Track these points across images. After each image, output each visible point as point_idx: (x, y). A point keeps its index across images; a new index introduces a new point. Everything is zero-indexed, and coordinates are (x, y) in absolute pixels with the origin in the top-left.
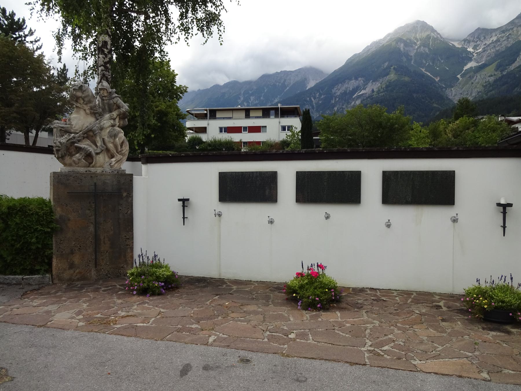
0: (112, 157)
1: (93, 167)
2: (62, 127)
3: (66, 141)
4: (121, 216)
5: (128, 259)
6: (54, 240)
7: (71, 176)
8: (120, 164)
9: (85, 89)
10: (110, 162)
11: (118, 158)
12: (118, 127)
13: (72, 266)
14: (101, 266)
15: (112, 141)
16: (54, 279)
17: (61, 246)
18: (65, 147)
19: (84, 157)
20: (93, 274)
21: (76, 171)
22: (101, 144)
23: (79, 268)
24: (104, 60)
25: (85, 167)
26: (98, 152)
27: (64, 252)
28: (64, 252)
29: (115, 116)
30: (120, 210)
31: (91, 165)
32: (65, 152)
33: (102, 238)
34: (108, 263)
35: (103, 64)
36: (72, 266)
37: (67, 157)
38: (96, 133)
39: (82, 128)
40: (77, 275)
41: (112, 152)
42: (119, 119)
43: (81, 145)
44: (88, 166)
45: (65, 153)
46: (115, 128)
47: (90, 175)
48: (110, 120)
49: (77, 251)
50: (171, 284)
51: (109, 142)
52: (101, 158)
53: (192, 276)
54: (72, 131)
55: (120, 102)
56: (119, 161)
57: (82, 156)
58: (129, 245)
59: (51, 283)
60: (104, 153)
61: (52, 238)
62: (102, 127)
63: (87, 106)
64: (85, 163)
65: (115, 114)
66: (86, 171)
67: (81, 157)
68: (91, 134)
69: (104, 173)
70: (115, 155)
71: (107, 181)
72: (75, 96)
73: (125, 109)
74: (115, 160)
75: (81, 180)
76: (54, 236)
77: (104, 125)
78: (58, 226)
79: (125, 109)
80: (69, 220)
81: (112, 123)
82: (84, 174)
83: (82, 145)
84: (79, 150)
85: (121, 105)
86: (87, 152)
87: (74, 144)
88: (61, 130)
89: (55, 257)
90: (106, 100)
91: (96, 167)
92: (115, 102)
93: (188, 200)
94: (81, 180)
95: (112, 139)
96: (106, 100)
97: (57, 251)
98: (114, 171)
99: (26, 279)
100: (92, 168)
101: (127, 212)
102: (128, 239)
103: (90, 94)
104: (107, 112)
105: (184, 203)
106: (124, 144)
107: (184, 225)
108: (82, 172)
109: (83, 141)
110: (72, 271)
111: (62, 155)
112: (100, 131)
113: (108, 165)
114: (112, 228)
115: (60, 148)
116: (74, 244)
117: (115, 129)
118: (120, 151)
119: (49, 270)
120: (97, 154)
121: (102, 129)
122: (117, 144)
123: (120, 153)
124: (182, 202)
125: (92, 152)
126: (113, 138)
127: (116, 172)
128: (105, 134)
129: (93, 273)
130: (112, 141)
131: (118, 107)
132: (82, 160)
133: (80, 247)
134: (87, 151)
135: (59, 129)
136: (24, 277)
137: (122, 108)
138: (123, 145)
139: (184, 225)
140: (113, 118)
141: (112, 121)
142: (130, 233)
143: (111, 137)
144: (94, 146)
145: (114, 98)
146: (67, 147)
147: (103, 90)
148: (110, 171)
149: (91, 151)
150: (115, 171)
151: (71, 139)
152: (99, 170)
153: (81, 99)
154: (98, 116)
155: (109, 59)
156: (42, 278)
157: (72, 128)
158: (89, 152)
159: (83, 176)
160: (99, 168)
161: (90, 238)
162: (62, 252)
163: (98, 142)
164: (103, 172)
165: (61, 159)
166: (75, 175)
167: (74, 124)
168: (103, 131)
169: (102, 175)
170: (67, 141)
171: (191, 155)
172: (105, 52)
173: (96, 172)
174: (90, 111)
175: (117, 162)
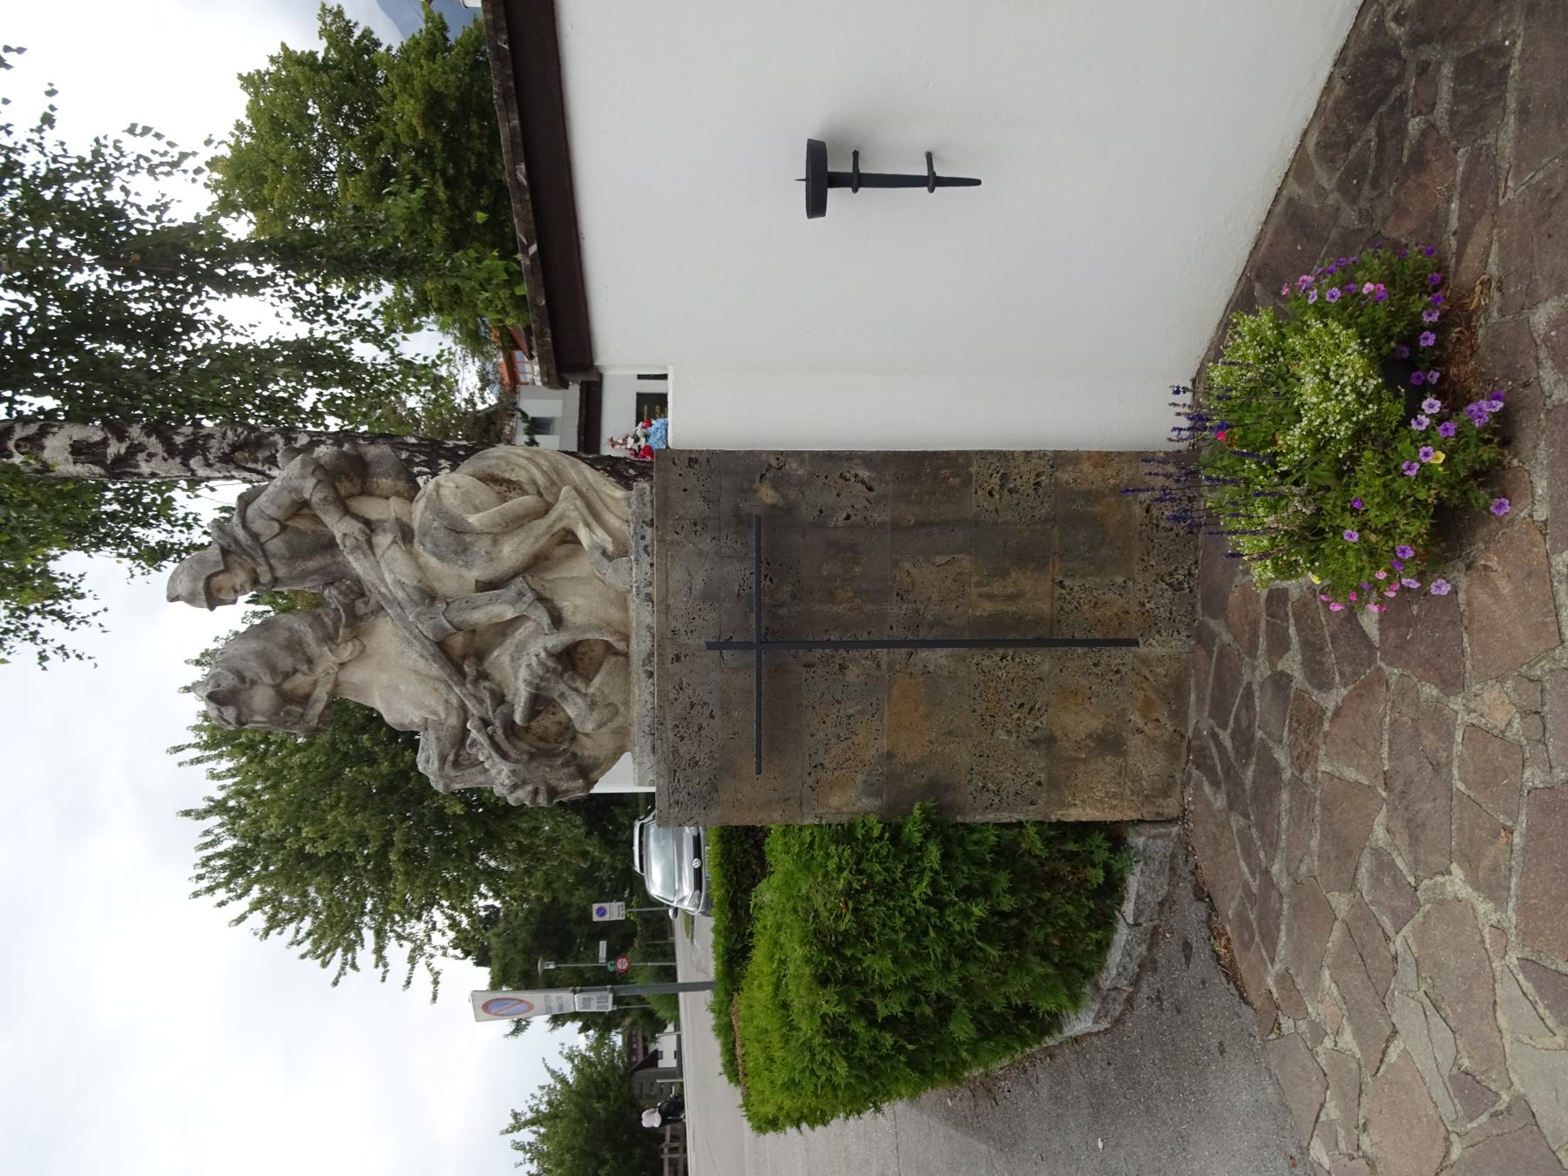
0: (568, 538)
1: (626, 638)
2: (443, 760)
3: (504, 762)
4: (882, 515)
5: (1112, 481)
6: (979, 818)
7: (675, 752)
8: (608, 500)
9: (231, 676)
10: (597, 555)
11: (574, 514)
12: (411, 499)
13: (1110, 743)
14: (1127, 612)
15: (484, 545)
16: (1158, 814)
17: (1012, 790)
18: (534, 764)
19: (579, 684)
20: (1160, 651)
21: (648, 720)
23: (1124, 709)
24: (159, 458)
25: (627, 682)
26: (545, 620)
27: (1043, 777)
28: (1043, 777)
29: (354, 527)
30: (848, 518)
31: (620, 646)
33: (988, 607)
34: (1119, 580)
35: (178, 460)
36: (1110, 743)
37: (583, 748)
38: (448, 626)
39: (438, 679)
40: (1157, 720)
41: (543, 541)
42: (371, 494)
43: (517, 690)
44: (622, 659)
45: (565, 765)
46: (416, 525)
47: (668, 665)
48: (379, 552)
49: (1044, 719)
50: (1417, 328)
51: (490, 557)
52: (579, 601)
53: (1305, 134)
54: (453, 720)
55: (272, 502)
56: (589, 506)
57: (574, 694)
58: (1038, 475)
59: (1175, 830)
60: (548, 581)
61: (971, 829)
62: (416, 597)
63: (321, 656)
64: (610, 673)
65: (340, 527)
66: (651, 675)
67: (579, 700)
68: (458, 642)
69: (653, 590)
70: (559, 526)
71: (699, 584)
72: (276, 713)
73: (303, 477)
74: (588, 525)
75: (692, 705)
76: (959, 819)
77: (402, 585)
78: (917, 812)
79: (303, 477)
80: (890, 756)
81: (394, 542)
82: (662, 694)
83: (520, 695)
84: (540, 702)
85: (286, 499)
86: (554, 671)
87: (514, 722)
88: (456, 764)
89: (1060, 812)
90: (272, 568)
91: (626, 623)
92: (276, 526)
93: (817, 153)
94: (692, 705)
95: (471, 544)
96: (272, 568)
97: (1032, 804)
98: (643, 543)
99: (1138, 913)
100: (633, 642)
101: (863, 482)
102: (1004, 477)
103: (254, 645)
104: (340, 559)
105: (838, 180)
106: (497, 472)
107: (977, 182)
108: (652, 694)
109: (498, 677)
110: (1134, 743)
111: (572, 778)
112: (441, 606)
113: (616, 570)
114: (939, 560)
115: (542, 788)
116: (1009, 732)
117: (422, 524)
118: (540, 494)
119: (1114, 834)
120: (557, 621)
121: (428, 596)
122: (498, 520)
123: (550, 499)
124: (834, 195)
125: (549, 645)
126: (468, 538)
127: (649, 532)
128: (454, 577)
129: (1154, 648)
130: (484, 545)
131: (300, 509)
132: (591, 690)
133: (1022, 705)
134: (548, 670)
135: (453, 774)
136: (1131, 921)
137: (299, 491)
138: (507, 476)
139: (977, 182)
140: (362, 538)
141: (383, 540)
142: (972, 470)
143: (465, 550)
144: (520, 634)
145: (255, 536)
146: (532, 756)
147: (219, 590)
148: (646, 560)
149: (543, 654)
150: (643, 537)
151: (491, 738)
152: (642, 617)
153: (287, 686)
154: (367, 603)
156: (1146, 864)
157: (442, 724)
158: (551, 663)
159: (672, 696)
160: (632, 614)
161: (986, 662)
162: (1039, 784)
163: (499, 616)
164: (649, 598)
165: (593, 775)
166: (671, 735)
167: (417, 713)
168: (436, 585)
169: (668, 606)
170: (504, 755)
171: (516, 122)
172: (123, 451)
173: (649, 628)
174: (346, 641)
175: (596, 515)
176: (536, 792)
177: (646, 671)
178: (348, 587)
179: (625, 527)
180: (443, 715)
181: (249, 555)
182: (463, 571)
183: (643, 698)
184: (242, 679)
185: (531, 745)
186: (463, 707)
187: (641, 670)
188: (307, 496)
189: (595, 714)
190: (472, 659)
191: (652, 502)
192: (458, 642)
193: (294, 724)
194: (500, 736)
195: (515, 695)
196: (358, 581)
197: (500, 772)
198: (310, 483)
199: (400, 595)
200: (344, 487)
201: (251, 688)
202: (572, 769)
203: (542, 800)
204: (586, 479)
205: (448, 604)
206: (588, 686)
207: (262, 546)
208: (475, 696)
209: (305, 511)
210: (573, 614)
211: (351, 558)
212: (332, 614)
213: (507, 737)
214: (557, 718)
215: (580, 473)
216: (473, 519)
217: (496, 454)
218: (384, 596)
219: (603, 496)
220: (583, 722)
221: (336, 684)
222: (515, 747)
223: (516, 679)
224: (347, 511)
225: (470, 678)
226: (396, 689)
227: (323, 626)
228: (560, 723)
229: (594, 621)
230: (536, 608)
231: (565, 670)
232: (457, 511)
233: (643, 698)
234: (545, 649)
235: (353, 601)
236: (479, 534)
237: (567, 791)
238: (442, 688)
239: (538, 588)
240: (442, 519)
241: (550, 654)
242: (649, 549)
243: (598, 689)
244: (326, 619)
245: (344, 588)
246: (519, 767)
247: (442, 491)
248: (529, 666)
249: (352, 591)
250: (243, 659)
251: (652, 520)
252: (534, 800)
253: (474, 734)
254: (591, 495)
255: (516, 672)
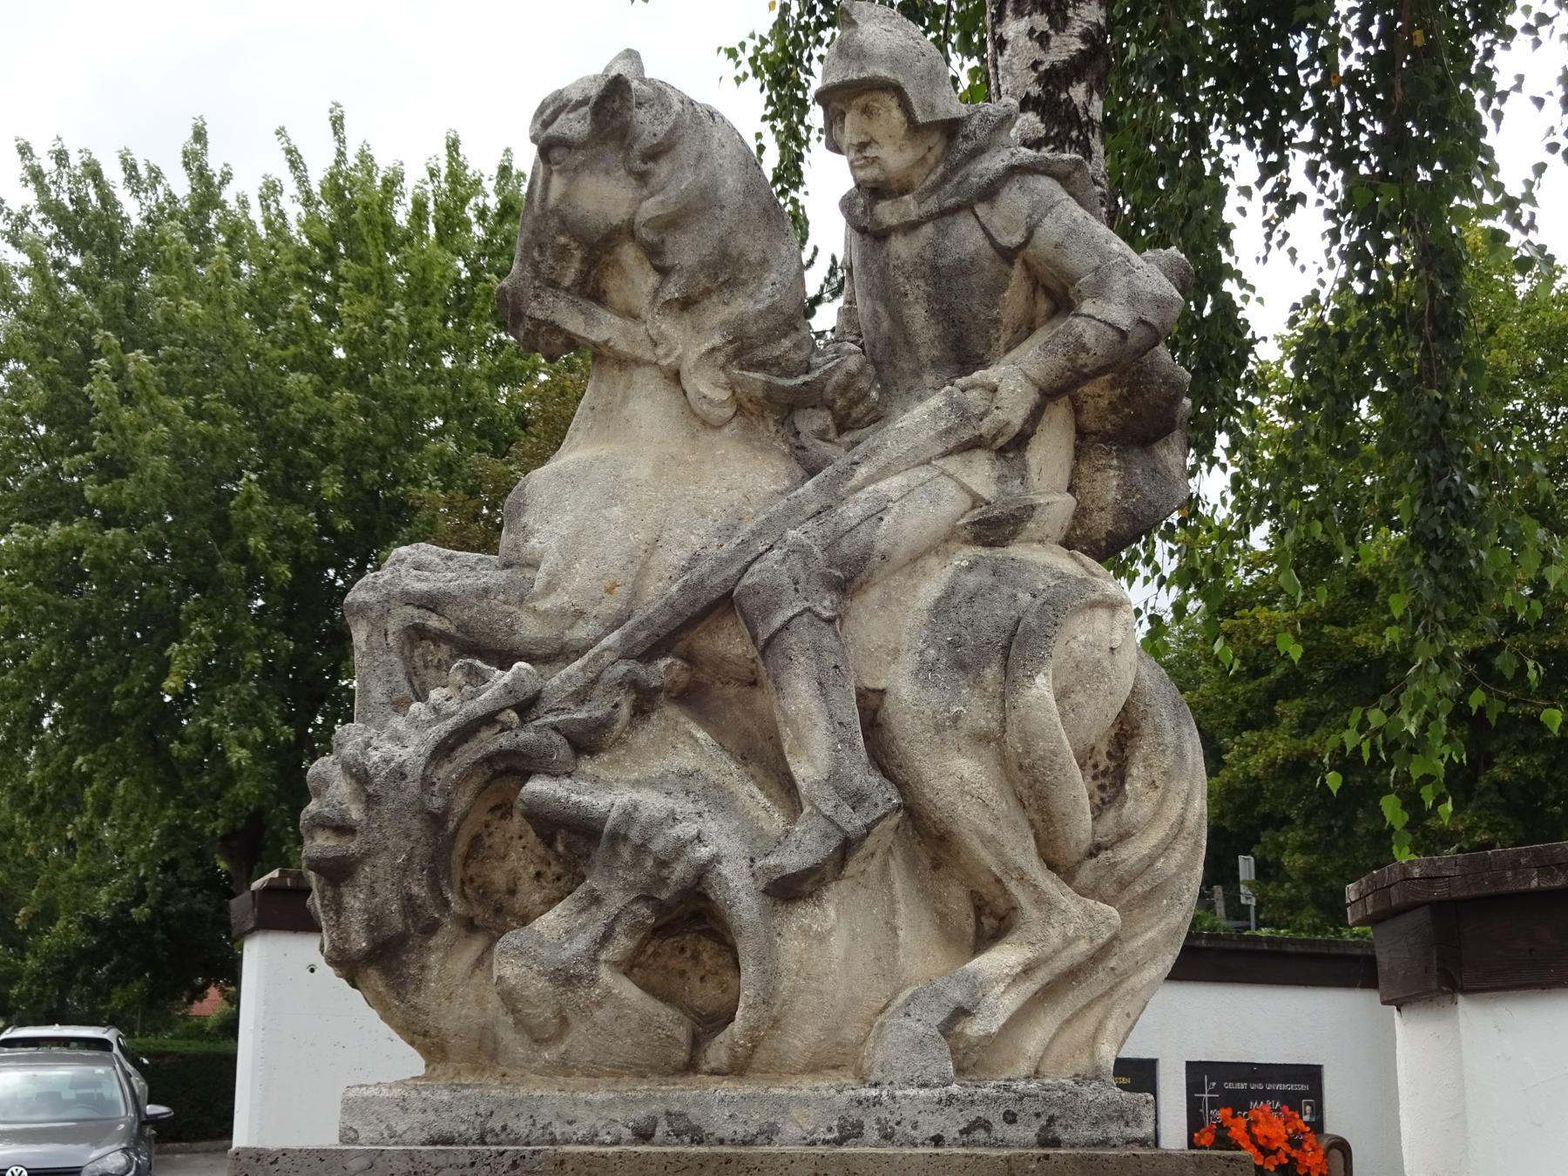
1: (738, 1068)
2: (430, 603)
3: (426, 750)
8: (1088, 1024)
9: (661, 130)
10: (957, 995)
11: (1054, 936)
12: (1068, 543)
18: (416, 825)
19: (622, 944)
21: (521, 1127)
22: (838, 761)
24: (1039, 55)
25: (623, 1069)
26: (792, 860)
29: (1013, 407)
31: (718, 1051)
32: (419, 890)
35: (1035, 90)
37: (449, 951)
38: (778, 621)
39: (635, 595)
41: (987, 857)
42: (1079, 454)
43: (609, 786)
44: (681, 1056)
45: (410, 905)
46: (1016, 551)
48: (952, 464)
51: (946, 725)
52: (837, 945)
54: (530, 629)
56: (1073, 975)
57: (597, 929)
60: (886, 864)
62: (846, 546)
63: (698, 329)
64: (646, 1024)
67: (581, 943)
68: (730, 643)
69: (867, 1148)
70: (1022, 897)
72: (565, 226)
73: (1133, 299)
74: (1028, 970)
77: (876, 516)
79: (1133, 299)
81: (977, 500)
85: (1077, 260)
87: (526, 776)
88: (416, 634)
90: (911, 227)
91: (778, 1069)
92: (1015, 239)
95: (978, 682)
96: (911, 227)
98: (995, 1117)
100: (727, 1088)
103: (731, 183)
104: (929, 379)
106: (1144, 747)
108: (591, 1139)
109: (641, 739)
111: (374, 923)
112: (825, 605)
113: (920, 1044)
115: (353, 846)
117: (1022, 566)
118: (1095, 850)
122: (1041, 746)
123: (1086, 874)
125: (726, 869)
126: (991, 673)
127: (1027, 1132)
130: (977, 712)
131: (1048, 292)
132: (605, 975)
134: (662, 864)
135: (393, 625)
138: (1136, 770)
140: (986, 427)
141: (981, 475)
143: (960, 665)
144: (752, 796)
145: (989, 192)
146: (436, 820)
147: (866, 111)
149: (703, 852)
150: (1010, 1118)
151: (489, 719)
153: (628, 254)
154: (822, 435)
155: (1085, 37)
157: (521, 601)
158: (679, 871)
160: (805, 1086)
164: (850, 1132)
165: (374, 976)
167: (553, 544)
168: (874, 595)
170: (443, 750)
173: (769, 1133)
174: (732, 386)
175: (1048, 993)
176: (343, 829)
177: (654, 1122)
178: (864, 395)
179: (1024, 1067)
180: (544, 605)
181: (944, 179)
182: (909, 661)
183: (581, 1112)
184: (654, 154)
185: (464, 817)
186: (560, 654)
187: (657, 1108)
188: (1087, 307)
189: (542, 984)
190: (684, 678)
191: (1104, 1143)
192: (730, 643)
193: (535, 266)
194: (493, 741)
195: (596, 780)
196: (877, 418)
197: (397, 738)
198: (1120, 314)
199: (852, 511)
200: (1098, 393)
201: (630, 172)
202: (397, 922)
203: (320, 844)
204: (1139, 967)
205: (830, 621)
206: (615, 965)
207: (966, 207)
208: (594, 681)
209: (1043, 305)
210: (805, 932)
211: (936, 401)
212: (797, 357)
213: (489, 759)
214: (526, 885)
215: (1154, 951)
216: (1042, 687)
217: (1188, 746)
218: (848, 472)
219: (1098, 1010)
220: (521, 953)
221: (625, 363)
222: (465, 778)
223: (636, 784)
224: (1048, 395)
225: (642, 671)
226: (612, 498)
227: (771, 337)
228: (512, 892)
229: (785, 984)
230: (826, 836)
231: (660, 908)
232: (1058, 650)
233: (581, 1112)
234: (716, 859)
235: (829, 406)
236: (1004, 700)
237: (337, 907)
238: (613, 605)
239: (870, 843)
240: (1041, 613)
241: (704, 871)
242: (980, 1135)
243: (608, 993)
244: (787, 343)
245: (863, 384)
246: (412, 787)
247: (1102, 615)
248: (673, 818)
249: (853, 403)
250: (700, 157)
251: (1056, 1143)
252: (322, 823)
253: (501, 678)
254: (1101, 975)
255: (650, 783)
